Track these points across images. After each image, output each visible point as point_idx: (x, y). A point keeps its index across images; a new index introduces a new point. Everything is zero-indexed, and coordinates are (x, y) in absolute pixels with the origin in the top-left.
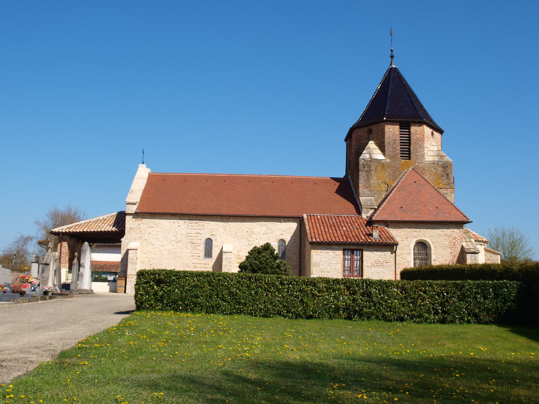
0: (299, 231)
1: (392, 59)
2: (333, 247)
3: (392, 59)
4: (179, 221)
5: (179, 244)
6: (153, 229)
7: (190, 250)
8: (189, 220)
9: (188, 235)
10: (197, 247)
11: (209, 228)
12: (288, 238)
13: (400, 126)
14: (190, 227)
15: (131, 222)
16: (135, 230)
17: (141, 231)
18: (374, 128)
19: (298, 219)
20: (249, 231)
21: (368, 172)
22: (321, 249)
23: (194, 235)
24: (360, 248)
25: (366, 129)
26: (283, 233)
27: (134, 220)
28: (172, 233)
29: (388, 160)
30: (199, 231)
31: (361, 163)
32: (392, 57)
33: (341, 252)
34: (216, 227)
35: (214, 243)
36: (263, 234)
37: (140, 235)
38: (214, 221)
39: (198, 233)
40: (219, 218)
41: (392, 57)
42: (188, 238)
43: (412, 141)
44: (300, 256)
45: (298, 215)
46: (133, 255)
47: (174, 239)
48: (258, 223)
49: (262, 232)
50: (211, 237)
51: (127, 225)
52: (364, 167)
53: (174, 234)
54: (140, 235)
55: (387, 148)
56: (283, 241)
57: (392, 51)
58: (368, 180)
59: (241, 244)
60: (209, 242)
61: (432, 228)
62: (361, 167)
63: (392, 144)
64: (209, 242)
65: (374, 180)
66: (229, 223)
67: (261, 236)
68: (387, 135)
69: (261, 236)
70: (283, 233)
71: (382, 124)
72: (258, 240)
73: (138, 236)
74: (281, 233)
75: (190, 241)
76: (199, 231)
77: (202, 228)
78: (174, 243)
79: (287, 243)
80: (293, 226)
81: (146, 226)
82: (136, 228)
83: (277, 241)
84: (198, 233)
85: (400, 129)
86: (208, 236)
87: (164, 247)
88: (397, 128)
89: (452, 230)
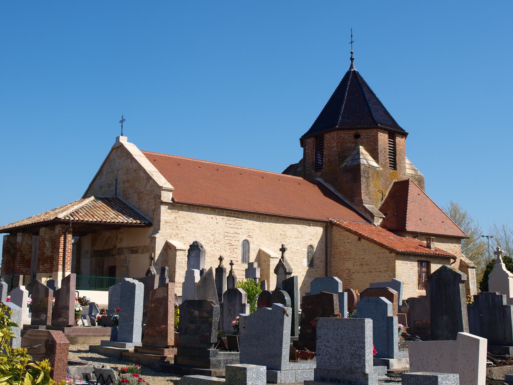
0: (324, 236)
1: (352, 62)
2: (411, 258)
3: (352, 62)
4: (218, 217)
5: (217, 245)
6: (190, 225)
8: (227, 216)
9: (226, 234)
10: (235, 250)
11: (248, 227)
12: (315, 244)
13: (389, 136)
14: (228, 225)
15: (166, 214)
16: (171, 224)
17: (177, 227)
18: (363, 133)
19: (325, 224)
20: (283, 233)
21: (368, 178)
22: (402, 260)
23: (232, 235)
24: (428, 259)
25: (352, 133)
26: (311, 238)
27: (170, 211)
28: (210, 231)
29: (381, 169)
30: (236, 230)
31: (362, 168)
32: (352, 59)
33: (416, 264)
34: (252, 227)
36: (295, 238)
38: (250, 219)
40: (256, 216)
41: (352, 59)
42: (226, 238)
43: (397, 152)
44: (326, 264)
46: (181, 257)
48: (290, 225)
49: (294, 236)
50: (248, 239)
51: (162, 218)
52: (364, 173)
53: (211, 232)
55: (381, 157)
56: (311, 246)
57: (352, 53)
58: (367, 187)
59: (275, 248)
60: (246, 244)
61: (442, 242)
62: (362, 174)
63: (383, 152)
64: (246, 244)
65: (372, 188)
66: (264, 223)
67: (293, 240)
68: (380, 143)
69: (293, 240)
70: (311, 238)
71: (375, 130)
72: (291, 244)
73: (174, 232)
76: (236, 230)
77: (240, 227)
78: (212, 244)
79: (315, 250)
80: (319, 231)
81: (182, 220)
82: (172, 221)
83: (307, 247)
85: (389, 138)
88: (386, 136)
89: (454, 245)
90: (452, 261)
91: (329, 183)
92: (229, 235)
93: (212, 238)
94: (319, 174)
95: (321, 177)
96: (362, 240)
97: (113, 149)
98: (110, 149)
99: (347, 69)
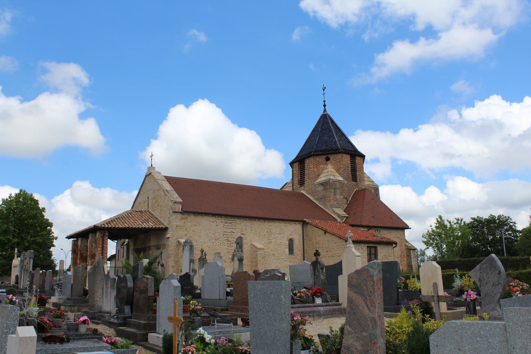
6: (196, 228)
7: (226, 247)
20: (269, 231)
25: (324, 157)
29: (346, 182)
32: (325, 106)
35: (244, 241)
37: (186, 233)
39: (232, 232)
42: (224, 236)
44: (304, 252)
45: (300, 219)
47: (213, 237)
50: (242, 236)
54: (186, 233)
57: (324, 101)
67: (277, 235)
74: (291, 233)
75: (226, 238)
78: (213, 240)
84: (232, 232)
86: (239, 235)
87: (205, 244)
90: (394, 245)
91: (309, 194)
92: (226, 233)
93: (213, 237)
94: (302, 188)
95: (304, 190)
96: (327, 233)
97: (146, 176)
98: (144, 177)
99: (321, 113)
